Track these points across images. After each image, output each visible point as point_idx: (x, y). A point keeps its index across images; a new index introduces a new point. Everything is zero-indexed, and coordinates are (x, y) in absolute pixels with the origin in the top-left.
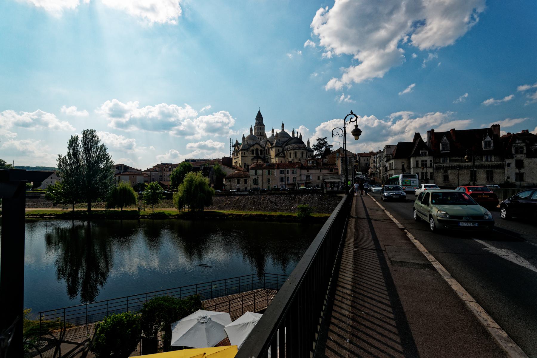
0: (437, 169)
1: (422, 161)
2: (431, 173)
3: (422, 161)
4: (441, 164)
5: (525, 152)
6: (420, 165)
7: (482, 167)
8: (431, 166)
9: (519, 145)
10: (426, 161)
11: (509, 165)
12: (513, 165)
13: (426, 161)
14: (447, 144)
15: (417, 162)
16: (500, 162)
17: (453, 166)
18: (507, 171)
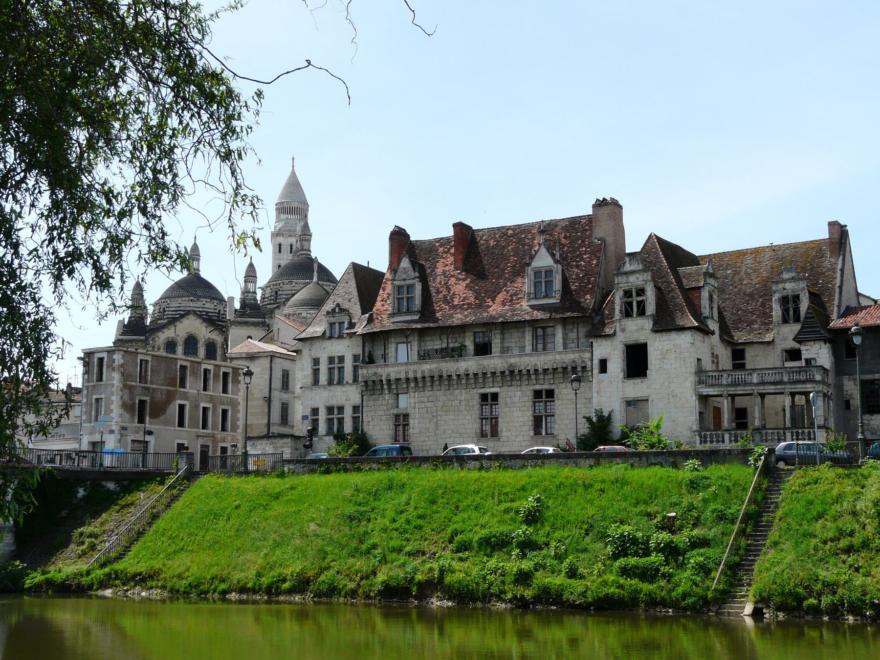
0: (372, 387)
1: (331, 360)
2: (356, 409)
3: (331, 360)
4: (380, 370)
5: (651, 308)
6: (323, 378)
7: (512, 375)
8: (355, 380)
9: (632, 278)
10: (341, 359)
11: (603, 366)
12: (617, 365)
13: (341, 359)
14: (410, 287)
15: (316, 361)
16: (571, 356)
17: (419, 375)
18: (598, 393)
